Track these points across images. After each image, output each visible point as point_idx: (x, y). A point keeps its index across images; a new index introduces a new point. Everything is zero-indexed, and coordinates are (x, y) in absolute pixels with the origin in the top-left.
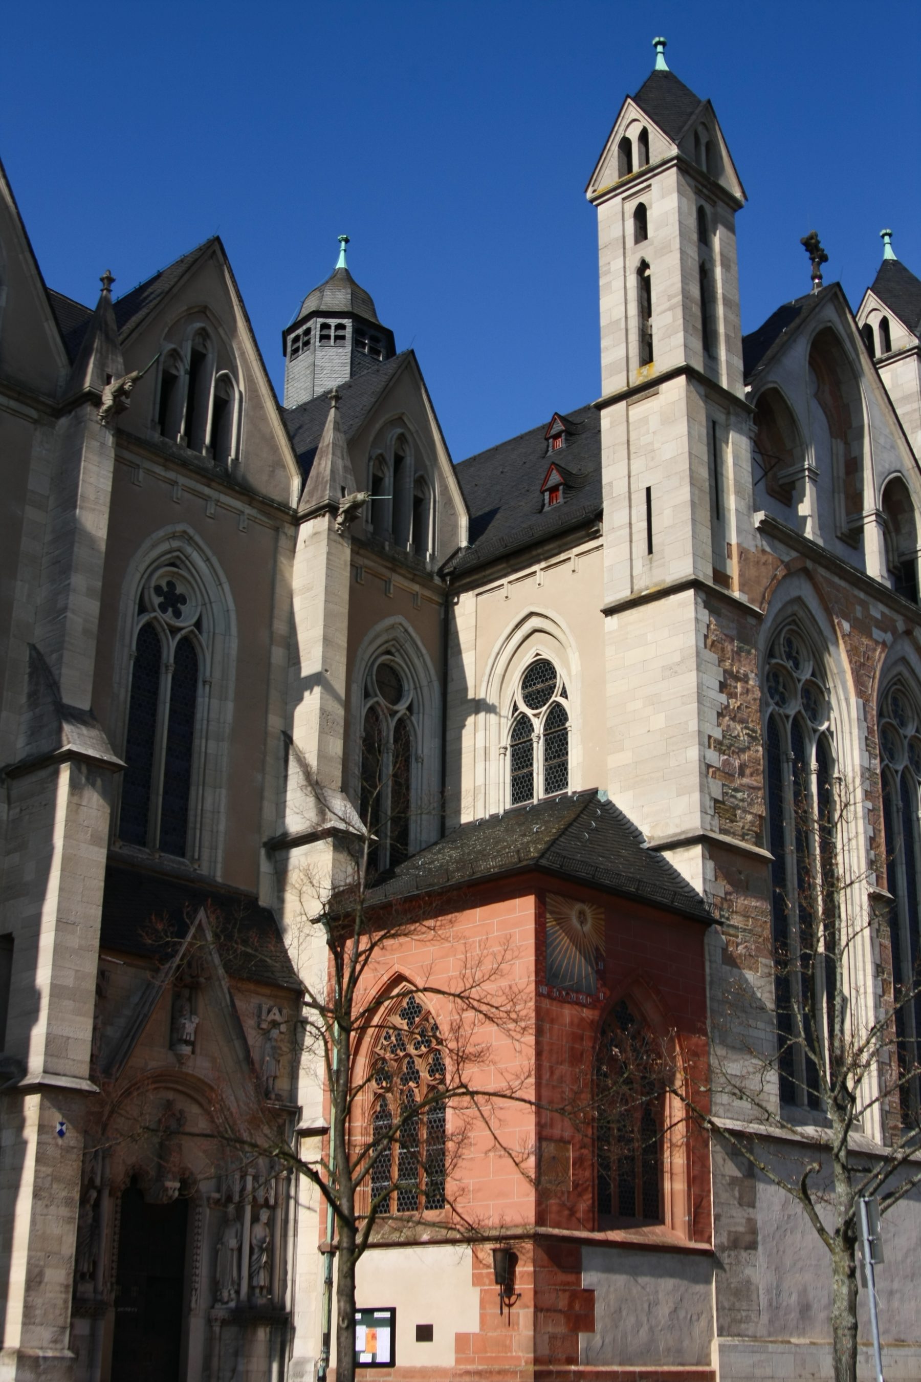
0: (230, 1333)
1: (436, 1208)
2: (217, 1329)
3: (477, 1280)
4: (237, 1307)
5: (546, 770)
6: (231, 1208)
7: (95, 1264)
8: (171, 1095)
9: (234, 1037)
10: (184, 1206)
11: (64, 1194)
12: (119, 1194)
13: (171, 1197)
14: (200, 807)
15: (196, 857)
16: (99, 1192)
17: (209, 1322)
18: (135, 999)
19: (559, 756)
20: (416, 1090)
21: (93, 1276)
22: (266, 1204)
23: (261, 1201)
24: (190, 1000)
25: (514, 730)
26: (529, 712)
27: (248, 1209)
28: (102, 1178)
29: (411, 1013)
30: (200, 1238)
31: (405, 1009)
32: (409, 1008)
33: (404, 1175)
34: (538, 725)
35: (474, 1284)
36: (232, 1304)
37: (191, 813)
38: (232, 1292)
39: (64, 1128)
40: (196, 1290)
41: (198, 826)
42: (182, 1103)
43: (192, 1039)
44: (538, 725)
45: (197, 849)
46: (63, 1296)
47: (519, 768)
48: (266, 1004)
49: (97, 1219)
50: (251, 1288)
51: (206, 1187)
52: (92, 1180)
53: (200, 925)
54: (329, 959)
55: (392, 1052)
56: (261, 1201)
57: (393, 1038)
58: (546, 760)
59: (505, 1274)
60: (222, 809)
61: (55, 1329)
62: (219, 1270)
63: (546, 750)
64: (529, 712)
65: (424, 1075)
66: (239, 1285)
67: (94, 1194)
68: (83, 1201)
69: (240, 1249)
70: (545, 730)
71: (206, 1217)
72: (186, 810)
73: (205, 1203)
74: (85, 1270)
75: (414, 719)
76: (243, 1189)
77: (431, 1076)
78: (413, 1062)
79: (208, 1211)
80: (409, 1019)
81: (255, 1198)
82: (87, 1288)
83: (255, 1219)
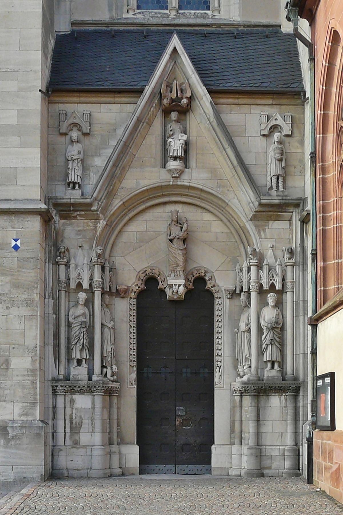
27: (253, 295)
36: (245, 378)
73: (224, 295)
79: (228, 300)
81: (261, 286)
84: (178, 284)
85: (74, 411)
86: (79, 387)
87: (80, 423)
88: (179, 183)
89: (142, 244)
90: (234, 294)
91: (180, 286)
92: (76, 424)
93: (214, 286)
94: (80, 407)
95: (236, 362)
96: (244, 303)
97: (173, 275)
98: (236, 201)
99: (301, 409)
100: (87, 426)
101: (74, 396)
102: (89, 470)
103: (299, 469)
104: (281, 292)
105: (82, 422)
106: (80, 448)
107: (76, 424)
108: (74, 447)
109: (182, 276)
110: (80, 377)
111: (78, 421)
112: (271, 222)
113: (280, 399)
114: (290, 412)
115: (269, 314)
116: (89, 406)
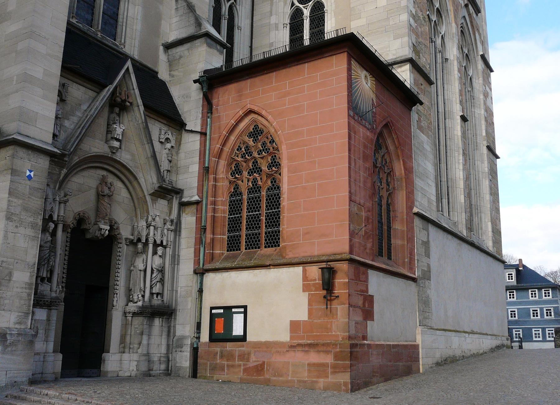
0: (138, 321)
1: (272, 247)
2: (130, 319)
3: (306, 288)
4: (143, 305)
5: (310, 34)
6: (140, 246)
7: (51, 272)
8: (105, 173)
9: (145, 143)
10: (112, 239)
11: (31, 219)
12: (69, 230)
13: (103, 235)
14: (126, 14)
15: (123, 41)
16: (56, 226)
17: (125, 313)
18: (84, 107)
19: (318, 27)
20: (259, 178)
21: (50, 280)
22: (161, 244)
23: (158, 242)
24: (119, 115)
25: (292, 16)
26: (301, 6)
27: (151, 246)
28: (58, 216)
29: (256, 134)
30: (120, 263)
31: (251, 132)
32: (254, 132)
33: (250, 228)
34: (307, 12)
35: (304, 291)
36: (140, 304)
37: (120, 17)
38: (140, 296)
39: (32, 174)
40: (117, 294)
41: (124, 24)
42: (111, 179)
43: (120, 138)
44: (307, 12)
45: (123, 37)
46: (27, 291)
47: (294, 35)
48: (164, 128)
49: (53, 242)
50: (152, 294)
51: (125, 232)
52: (51, 216)
53: (128, 68)
54: (203, 106)
55: (242, 157)
56: (158, 242)
57: (243, 149)
58: (310, 29)
59: (328, 285)
60: (139, 18)
61: (20, 314)
62: (131, 282)
63: (310, 24)
64: (301, 6)
65: (264, 168)
66: (144, 292)
67: (52, 226)
68: (45, 229)
69: (145, 271)
70: (310, 14)
71: (123, 251)
72: (117, 15)
73: (124, 242)
74: (45, 276)
75: (238, 7)
76: (148, 235)
77: (269, 169)
78: (257, 162)
79: (125, 246)
80: (254, 138)
81: (155, 241)
82: (45, 288)
83: (155, 253)
88: (114, 157)
90: (132, 243)
93: (118, 234)
95: (129, 292)
97: (103, 222)
98: (143, 180)
99: (172, 328)
100: (41, 335)
103: (168, 371)
104: (165, 247)
109: (109, 224)
110: (45, 293)
112: (159, 199)
114: (165, 329)
115: (157, 261)
116: (44, 317)
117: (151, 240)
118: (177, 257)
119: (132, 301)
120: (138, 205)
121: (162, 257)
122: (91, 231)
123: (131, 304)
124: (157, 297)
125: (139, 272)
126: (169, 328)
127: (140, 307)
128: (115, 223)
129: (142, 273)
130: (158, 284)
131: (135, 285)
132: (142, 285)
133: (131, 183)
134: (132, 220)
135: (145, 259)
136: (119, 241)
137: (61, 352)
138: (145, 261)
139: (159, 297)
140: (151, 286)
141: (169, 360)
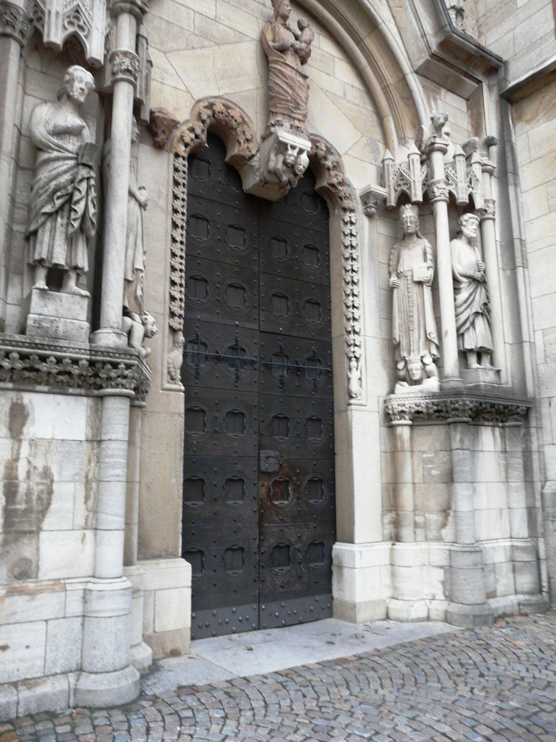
0: (430, 439)
2: (405, 432)
4: (441, 388)
6: (409, 213)
17: (388, 418)
22: (470, 207)
27: (442, 210)
36: (432, 384)
38: (428, 360)
50: (464, 354)
51: (358, 175)
62: (397, 321)
66: (439, 348)
71: (362, 238)
74: (60, 257)
83: (456, 233)
84: (299, 146)
85: (25, 450)
86: (59, 361)
87: (45, 496)
89: (206, 43)
91: (301, 151)
92: (28, 500)
94: (48, 436)
95: (393, 349)
96: (413, 225)
97: (287, 124)
99: (535, 457)
100: (69, 505)
101: (27, 398)
102: (72, 678)
103: (541, 591)
105: (50, 492)
106: (40, 591)
107: (28, 500)
108: (21, 592)
111: (36, 489)
112: (443, 91)
113: (494, 435)
114: (518, 462)
117: (440, 191)
118: (517, 243)
119: (404, 380)
120: (386, 99)
121: (479, 242)
122: (255, 162)
123: (402, 388)
124: (479, 361)
125: (415, 289)
126: (527, 454)
127: (434, 395)
128: (329, 150)
129: (427, 291)
130: (480, 323)
131: (409, 330)
132: (431, 327)
133: (359, 42)
134: (375, 151)
135: (429, 251)
136: (346, 203)
137: (187, 555)
138: (429, 257)
139: (486, 360)
140: (458, 330)
141: (538, 559)
